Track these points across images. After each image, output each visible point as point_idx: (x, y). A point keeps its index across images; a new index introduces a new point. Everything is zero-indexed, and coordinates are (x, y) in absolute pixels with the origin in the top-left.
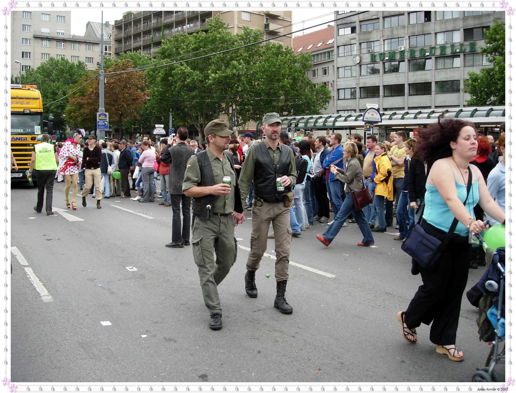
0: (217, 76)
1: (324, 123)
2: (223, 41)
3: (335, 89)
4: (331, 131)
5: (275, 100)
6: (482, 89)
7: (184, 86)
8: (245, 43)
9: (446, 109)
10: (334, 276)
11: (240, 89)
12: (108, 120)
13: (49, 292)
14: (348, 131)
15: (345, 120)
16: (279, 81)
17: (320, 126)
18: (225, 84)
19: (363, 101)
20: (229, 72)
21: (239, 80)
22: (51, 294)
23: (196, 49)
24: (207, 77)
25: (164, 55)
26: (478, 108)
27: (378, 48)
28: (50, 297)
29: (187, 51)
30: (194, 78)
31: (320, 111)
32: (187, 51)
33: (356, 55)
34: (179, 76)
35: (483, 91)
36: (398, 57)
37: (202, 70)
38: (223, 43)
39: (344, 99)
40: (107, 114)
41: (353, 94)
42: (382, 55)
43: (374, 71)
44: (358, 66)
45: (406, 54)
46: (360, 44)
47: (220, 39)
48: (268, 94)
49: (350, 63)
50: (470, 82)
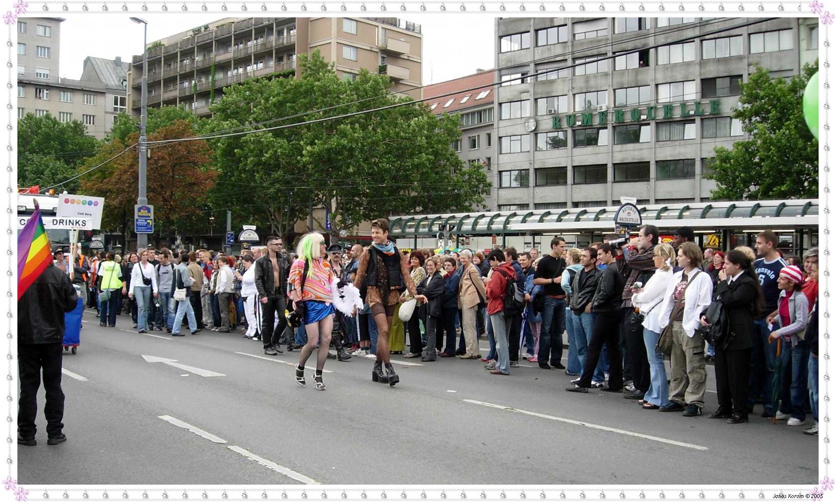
1: (505, 227)
2: (325, 92)
3: (496, 172)
4: (499, 240)
5: (401, 188)
6: (737, 173)
8: (359, 96)
9: (685, 205)
10: (705, 448)
11: (351, 170)
12: (152, 217)
14: (529, 239)
15: (524, 221)
16: (411, 156)
18: (328, 162)
19: (538, 190)
20: (334, 142)
21: (352, 156)
23: (280, 104)
25: (226, 113)
26: (737, 203)
27: (563, 106)
30: (276, 152)
32: (266, 108)
33: (530, 118)
34: (252, 146)
35: (737, 177)
36: (596, 121)
38: (324, 95)
39: (510, 187)
40: (152, 207)
41: (523, 178)
42: (571, 118)
43: (557, 144)
44: (532, 134)
45: (610, 117)
46: (536, 100)
47: (319, 91)
48: (394, 178)
49: (519, 130)
50: (718, 162)
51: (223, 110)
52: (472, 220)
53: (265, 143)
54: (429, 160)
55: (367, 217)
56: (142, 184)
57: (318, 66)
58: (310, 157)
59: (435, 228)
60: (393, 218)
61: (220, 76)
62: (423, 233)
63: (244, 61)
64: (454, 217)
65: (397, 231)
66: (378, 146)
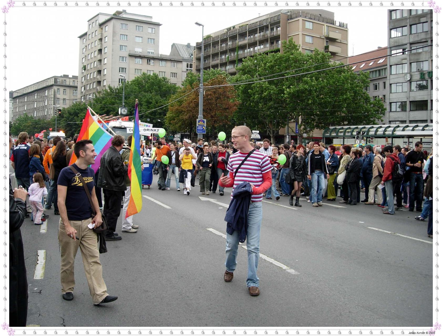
0: (292, 91)
2: (296, 61)
3: (388, 103)
4: (390, 140)
7: (261, 98)
11: (310, 102)
12: (205, 126)
13: (288, 267)
14: (406, 140)
15: (403, 130)
16: (342, 94)
17: (380, 135)
18: (297, 97)
22: (291, 268)
23: (271, 67)
24: (282, 91)
25: (244, 71)
28: (294, 271)
29: (265, 69)
30: (270, 92)
31: (377, 121)
33: (407, 73)
37: (276, 85)
38: (295, 62)
39: (396, 111)
40: (205, 120)
41: (403, 106)
44: (409, 82)
46: (411, 63)
47: (293, 60)
49: (401, 80)
51: (243, 70)
52: (375, 129)
53: (264, 88)
54: (351, 96)
55: (318, 127)
56: (201, 108)
57: (292, 47)
58: (288, 94)
59: (355, 133)
60: (331, 128)
61: (241, 52)
62: (347, 136)
63: (253, 44)
64: (365, 128)
65: (334, 134)
66: (324, 89)
